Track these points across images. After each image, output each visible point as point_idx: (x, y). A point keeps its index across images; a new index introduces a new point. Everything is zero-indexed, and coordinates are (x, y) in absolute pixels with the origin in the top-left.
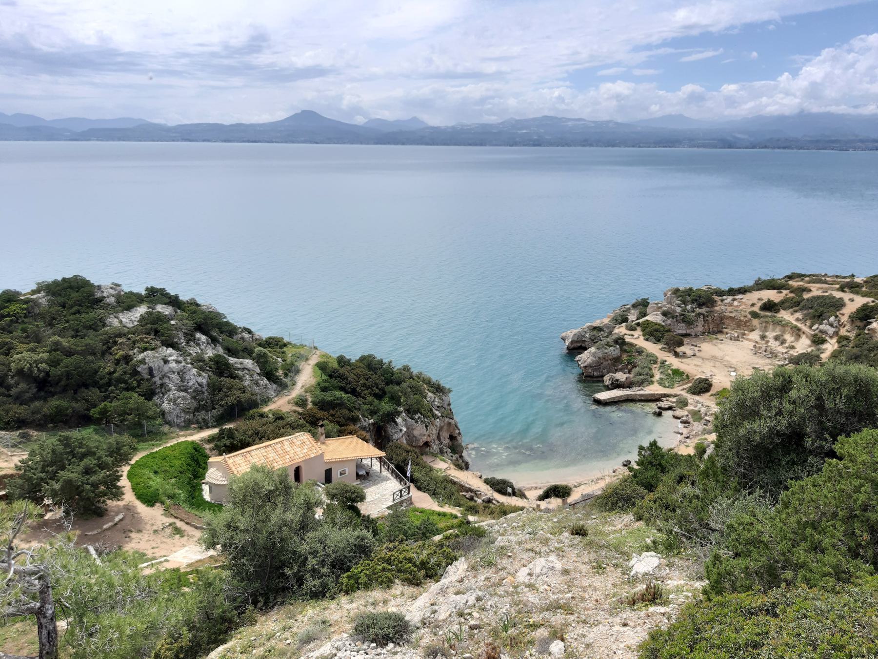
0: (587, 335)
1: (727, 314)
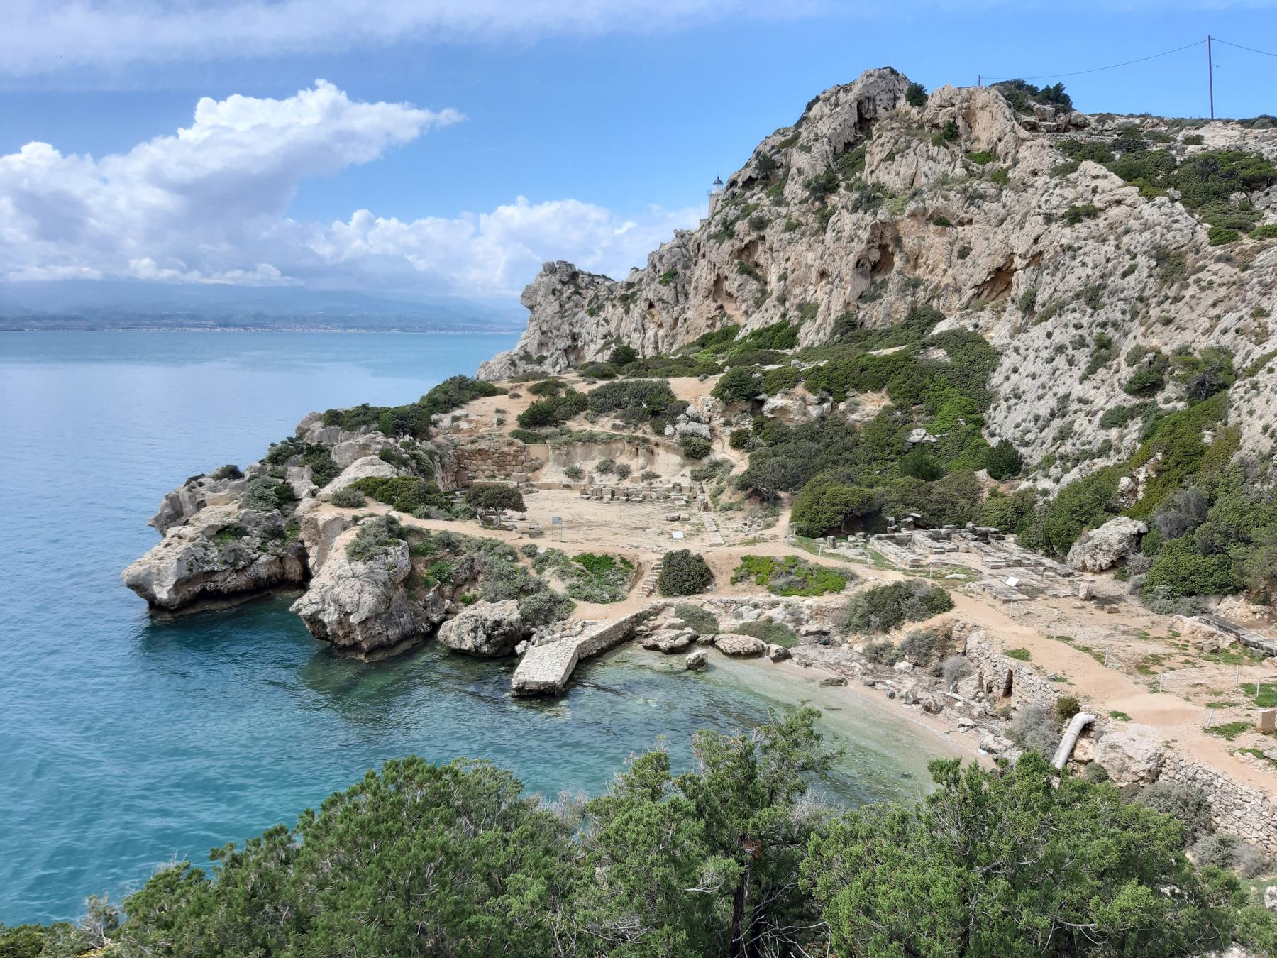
0: (214, 554)
1: (468, 447)
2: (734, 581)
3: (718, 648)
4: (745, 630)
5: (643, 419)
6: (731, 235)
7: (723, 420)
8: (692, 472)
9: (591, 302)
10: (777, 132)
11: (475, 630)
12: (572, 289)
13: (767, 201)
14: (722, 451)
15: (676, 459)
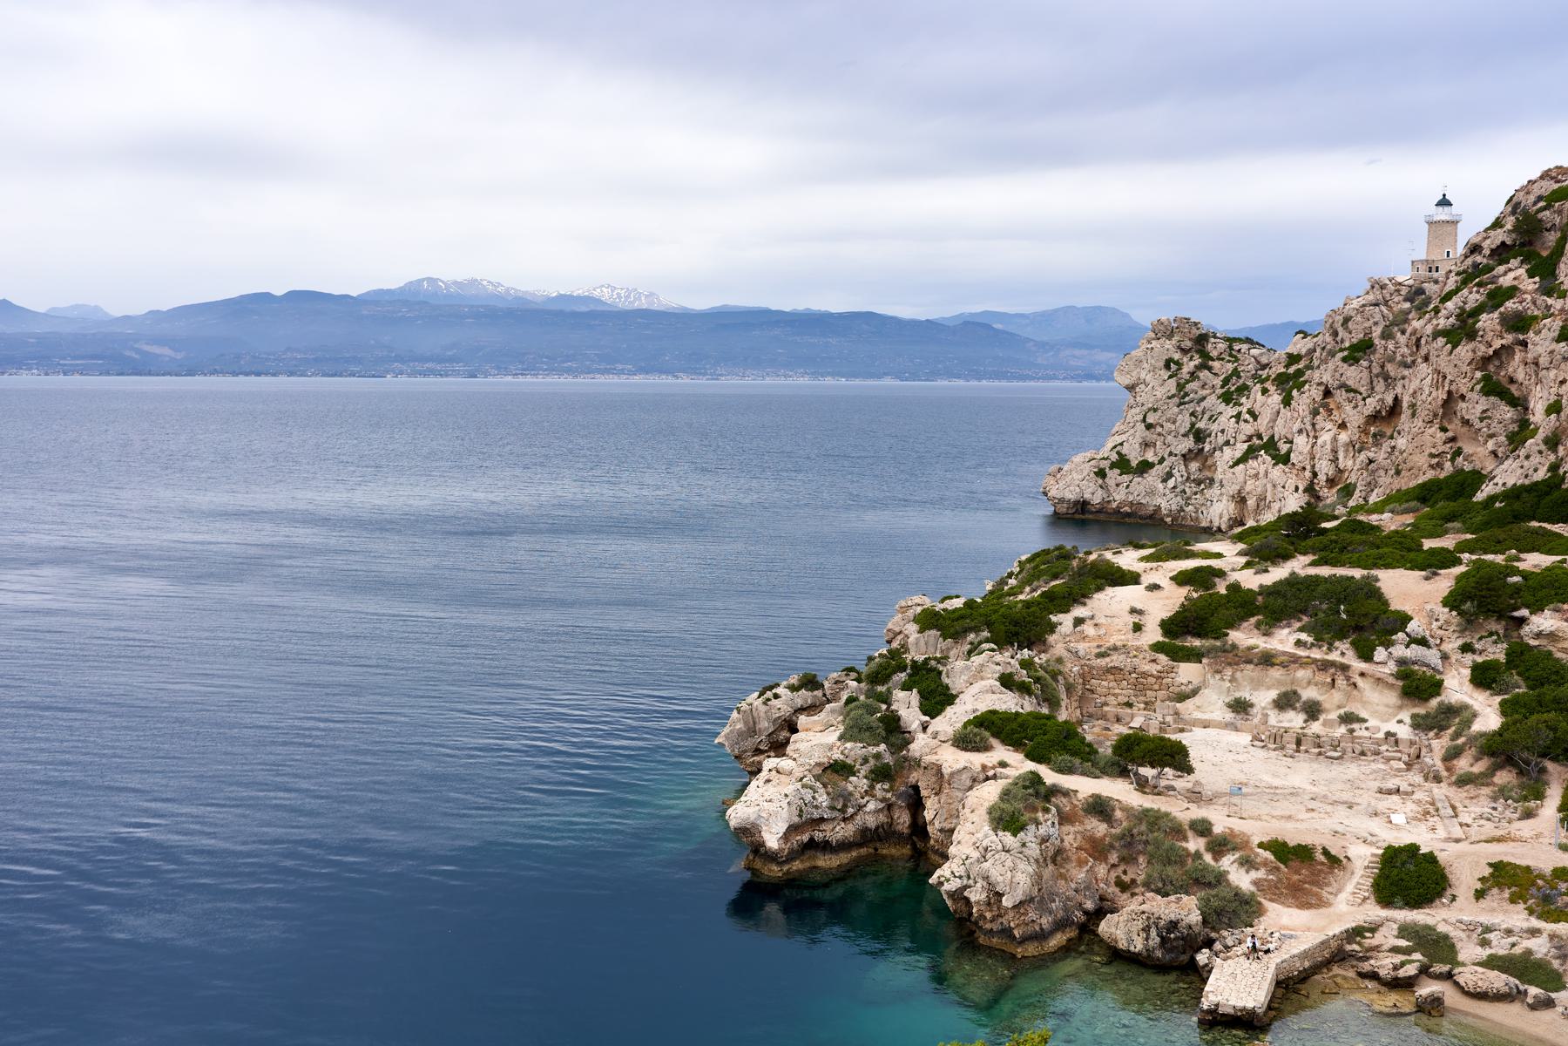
2: (1480, 895)
3: (1457, 984)
4: (1492, 963)
5: (1341, 636)
6: (1472, 335)
7: (1460, 642)
8: (1414, 717)
9: (1226, 381)
10: (1546, 175)
11: (1146, 929)
12: (1197, 361)
13: (1530, 285)
14: (1457, 687)
15: (1392, 698)
